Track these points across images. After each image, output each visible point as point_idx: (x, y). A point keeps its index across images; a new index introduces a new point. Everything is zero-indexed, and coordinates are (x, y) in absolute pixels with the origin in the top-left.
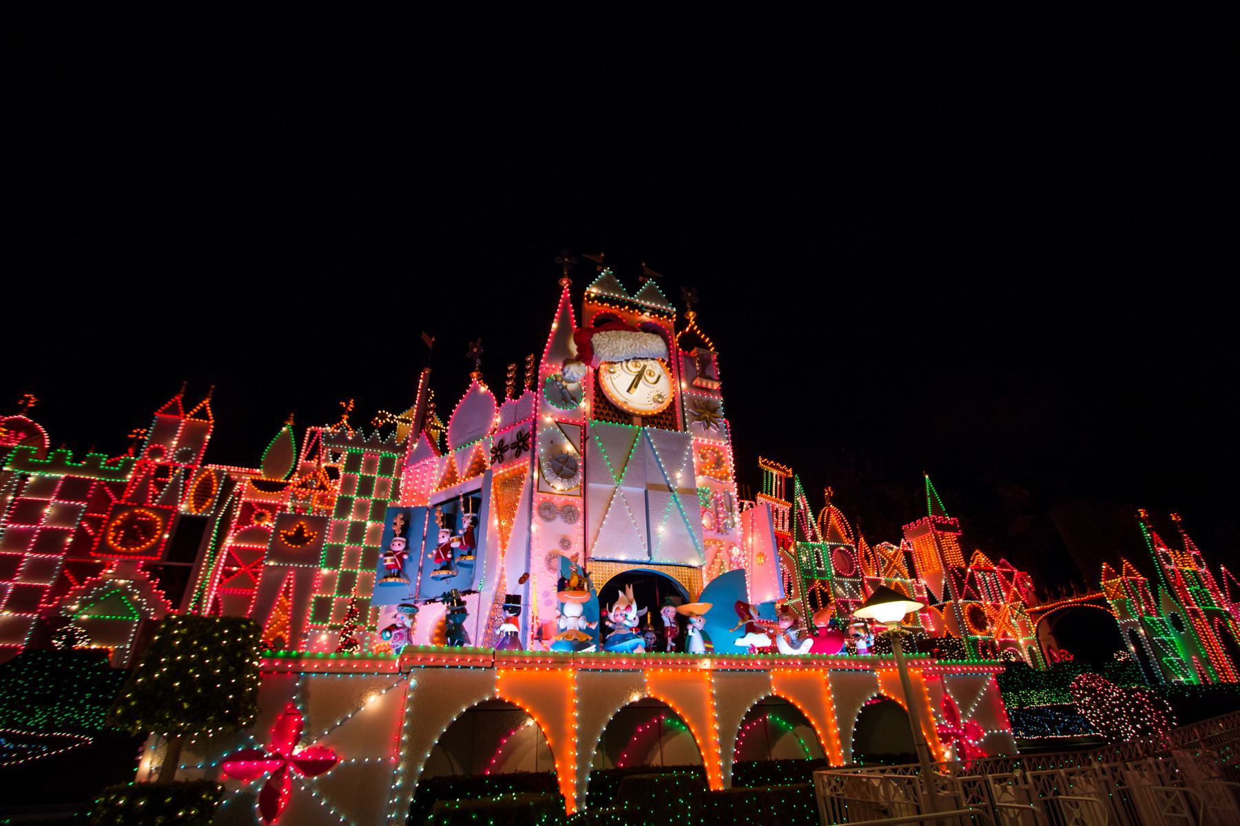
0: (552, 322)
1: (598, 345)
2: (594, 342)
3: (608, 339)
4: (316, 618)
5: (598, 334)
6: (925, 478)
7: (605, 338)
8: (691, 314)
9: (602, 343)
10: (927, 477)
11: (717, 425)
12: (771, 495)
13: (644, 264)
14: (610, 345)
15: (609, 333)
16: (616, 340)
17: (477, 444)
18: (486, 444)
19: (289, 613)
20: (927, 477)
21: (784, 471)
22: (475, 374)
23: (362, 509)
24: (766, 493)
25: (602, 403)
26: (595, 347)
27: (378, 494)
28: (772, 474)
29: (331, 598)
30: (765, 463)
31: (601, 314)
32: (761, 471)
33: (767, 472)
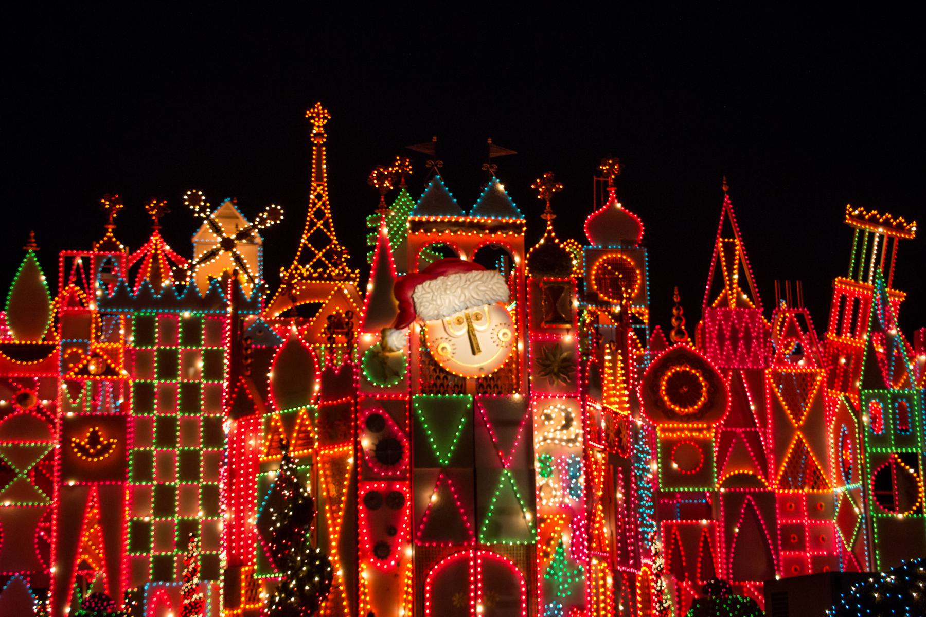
2: (416, 300)
4: (134, 548)
5: (419, 287)
7: (429, 293)
11: (568, 376)
12: (865, 279)
13: (490, 142)
14: (434, 303)
15: (434, 282)
16: (441, 294)
17: (302, 410)
18: (310, 413)
19: (101, 545)
21: (900, 227)
23: (167, 397)
24: (855, 277)
26: (418, 306)
27: (185, 375)
28: (872, 235)
29: (172, 556)
30: (860, 217)
32: (852, 230)
33: (862, 232)
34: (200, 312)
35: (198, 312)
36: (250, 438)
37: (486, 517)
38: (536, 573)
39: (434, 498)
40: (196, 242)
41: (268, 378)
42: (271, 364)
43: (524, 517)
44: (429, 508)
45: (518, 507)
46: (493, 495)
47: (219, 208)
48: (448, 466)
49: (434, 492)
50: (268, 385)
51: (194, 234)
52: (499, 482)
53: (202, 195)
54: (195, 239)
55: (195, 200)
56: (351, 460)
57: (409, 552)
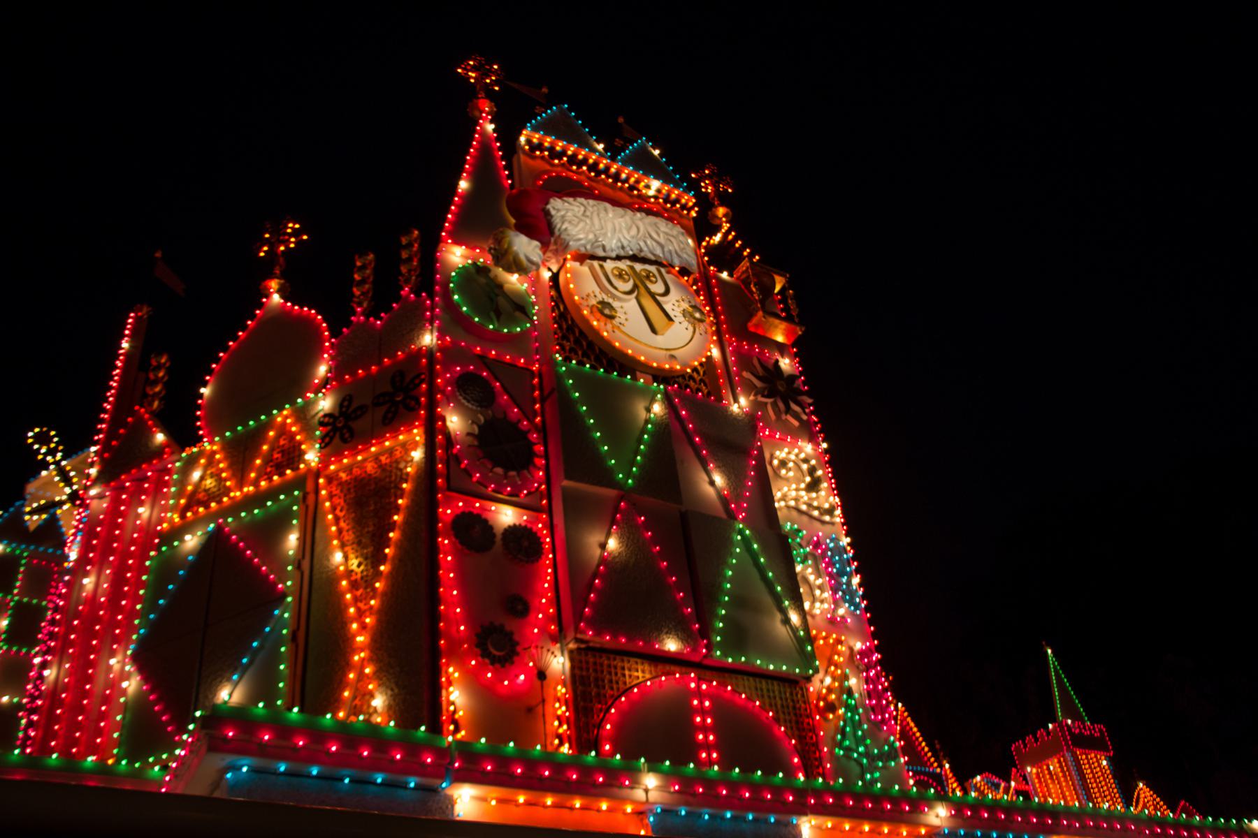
0: (458, 178)
1: (563, 217)
2: (553, 212)
3: (582, 209)
6: (1046, 652)
8: (721, 211)
9: (569, 214)
10: (1049, 651)
20: (1049, 651)
22: (274, 285)
25: (568, 340)
31: (550, 177)
34: (23, 547)
35: (18, 546)
36: (141, 504)
37: (717, 602)
38: (817, 746)
39: (613, 544)
40: (30, 494)
41: (201, 396)
42: (210, 372)
43: (787, 621)
44: (603, 560)
45: (768, 600)
46: (722, 563)
47: (61, 523)
48: (632, 489)
49: (608, 535)
50: (199, 407)
51: (32, 479)
52: (729, 543)
53: (54, 436)
54: (31, 488)
55: (43, 439)
56: (418, 455)
57: (558, 663)
